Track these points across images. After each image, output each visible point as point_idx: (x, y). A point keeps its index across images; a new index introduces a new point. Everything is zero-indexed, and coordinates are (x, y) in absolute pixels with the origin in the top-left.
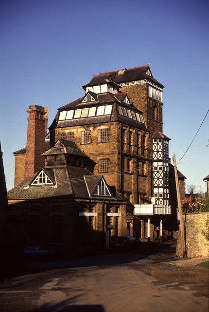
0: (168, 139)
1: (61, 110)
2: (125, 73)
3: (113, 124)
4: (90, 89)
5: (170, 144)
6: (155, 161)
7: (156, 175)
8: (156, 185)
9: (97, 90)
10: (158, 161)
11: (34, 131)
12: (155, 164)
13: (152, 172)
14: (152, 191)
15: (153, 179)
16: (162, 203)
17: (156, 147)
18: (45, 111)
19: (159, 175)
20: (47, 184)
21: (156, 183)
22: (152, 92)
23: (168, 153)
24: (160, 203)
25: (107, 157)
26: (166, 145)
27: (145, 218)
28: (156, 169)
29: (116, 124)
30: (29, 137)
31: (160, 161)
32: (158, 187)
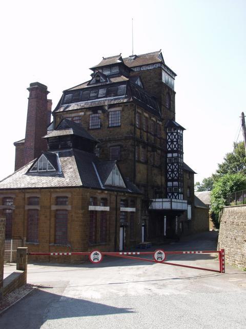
0: (183, 129)
1: (66, 92)
4: (101, 71)
6: (170, 152)
8: (170, 178)
11: (34, 113)
12: (169, 155)
13: (167, 164)
14: (167, 184)
15: (167, 172)
17: (171, 137)
21: (170, 175)
24: (174, 197)
25: (120, 143)
27: (162, 212)
31: (175, 152)
32: (173, 180)
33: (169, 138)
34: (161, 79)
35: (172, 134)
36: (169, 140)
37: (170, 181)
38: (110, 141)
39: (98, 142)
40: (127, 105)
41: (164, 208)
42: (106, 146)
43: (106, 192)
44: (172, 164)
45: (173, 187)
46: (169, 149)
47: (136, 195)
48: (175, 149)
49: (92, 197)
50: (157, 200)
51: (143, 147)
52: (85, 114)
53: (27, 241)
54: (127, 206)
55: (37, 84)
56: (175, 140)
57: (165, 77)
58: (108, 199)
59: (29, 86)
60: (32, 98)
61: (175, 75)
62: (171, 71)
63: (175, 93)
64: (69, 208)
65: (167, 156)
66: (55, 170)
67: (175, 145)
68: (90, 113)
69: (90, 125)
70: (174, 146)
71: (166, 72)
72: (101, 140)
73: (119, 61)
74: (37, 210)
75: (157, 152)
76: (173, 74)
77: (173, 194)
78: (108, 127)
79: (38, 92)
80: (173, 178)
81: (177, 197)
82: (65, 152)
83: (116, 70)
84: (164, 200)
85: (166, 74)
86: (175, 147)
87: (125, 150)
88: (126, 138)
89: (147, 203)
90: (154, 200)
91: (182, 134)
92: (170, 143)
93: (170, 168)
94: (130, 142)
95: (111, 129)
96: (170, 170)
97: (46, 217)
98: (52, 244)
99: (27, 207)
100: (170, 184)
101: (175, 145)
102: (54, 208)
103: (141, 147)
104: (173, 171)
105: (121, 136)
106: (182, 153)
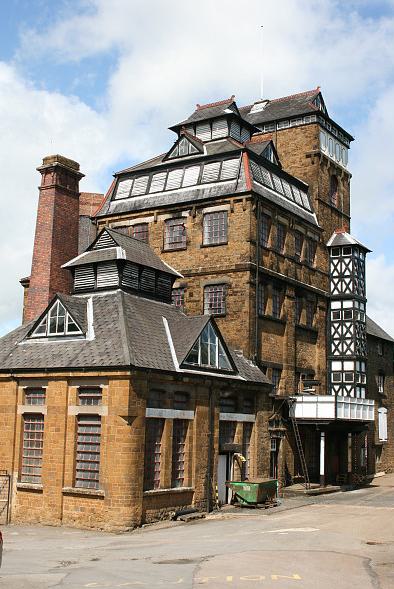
0: (365, 251)
1: (121, 177)
2: (266, 109)
3: (241, 200)
4: (191, 131)
5: (371, 264)
6: (336, 299)
7: (337, 330)
8: (337, 353)
9: (204, 135)
10: (342, 298)
12: (335, 305)
13: (328, 324)
15: (330, 340)
16: (352, 394)
18: (81, 171)
19: (339, 330)
20: (68, 333)
21: (338, 348)
22: (328, 147)
23: (364, 281)
24: (345, 394)
26: (359, 264)
28: (337, 315)
29: (247, 199)
30: (39, 228)
31: (348, 298)
32: (342, 359)
33: (336, 269)
34: (318, 146)
35: (341, 260)
36: (336, 274)
37: (337, 359)
38: (204, 274)
39: (180, 277)
40: (241, 200)
41: (319, 416)
42: (198, 286)
43: (186, 380)
44: (342, 323)
45: (343, 371)
46: (336, 292)
47: (254, 388)
48: (348, 292)
49: (153, 390)
50: (306, 399)
51: (274, 288)
52: (156, 222)
53: (19, 480)
54: (237, 410)
55: (58, 158)
56: (347, 273)
57: (328, 147)
58: (193, 394)
59: (40, 164)
60: (47, 188)
61: (351, 139)
62: (340, 129)
63: (347, 176)
64: (102, 410)
65: (329, 305)
66: (80, 332)
67: (348, 285)
68: (168, 216)
69: (167, 241)
70: (344, 287)
71: (328, 132)
72: (188, 275)
73: (228, 111)
74: (40, 416)
75: (306, 298)
76: (344, 138)
77: (343, 386)
78: (203, 247)
79: (63, 176)
80: (343, 353)
81: (352, 394)
82: (106, 297)
83: (221, 131)
84: (321, 399)
85: (329, 136)
86: (348, 288)
87: (235, 294)
88: (238, 269)
89: (284, 407)
90: (299, 399)
91: (364, 262)
92: (336, 280)
93: (336, 331)
94: (247, 276)
95: (207, 250)
96: (336, 336)
97: (58, 430)
98: (67, 488)
99: (22, 409)
100: (336, 366)
101: (348, 285)
102: (74, 410)
103: (270, 287)
104: (342, 339)
105: (226, 264)
106: (364, 301)
